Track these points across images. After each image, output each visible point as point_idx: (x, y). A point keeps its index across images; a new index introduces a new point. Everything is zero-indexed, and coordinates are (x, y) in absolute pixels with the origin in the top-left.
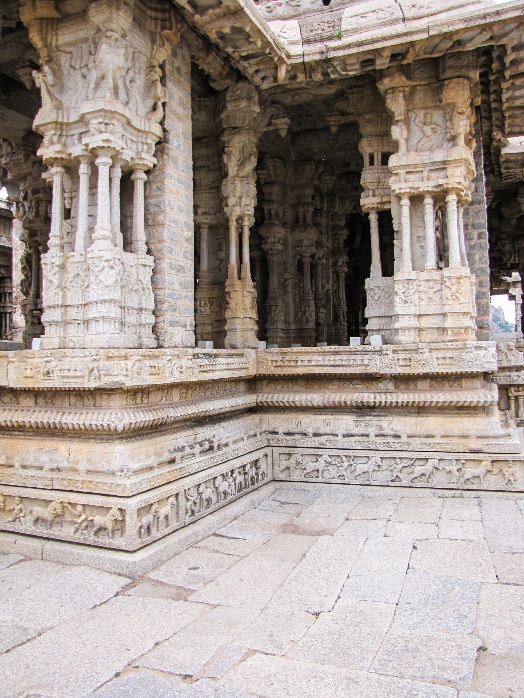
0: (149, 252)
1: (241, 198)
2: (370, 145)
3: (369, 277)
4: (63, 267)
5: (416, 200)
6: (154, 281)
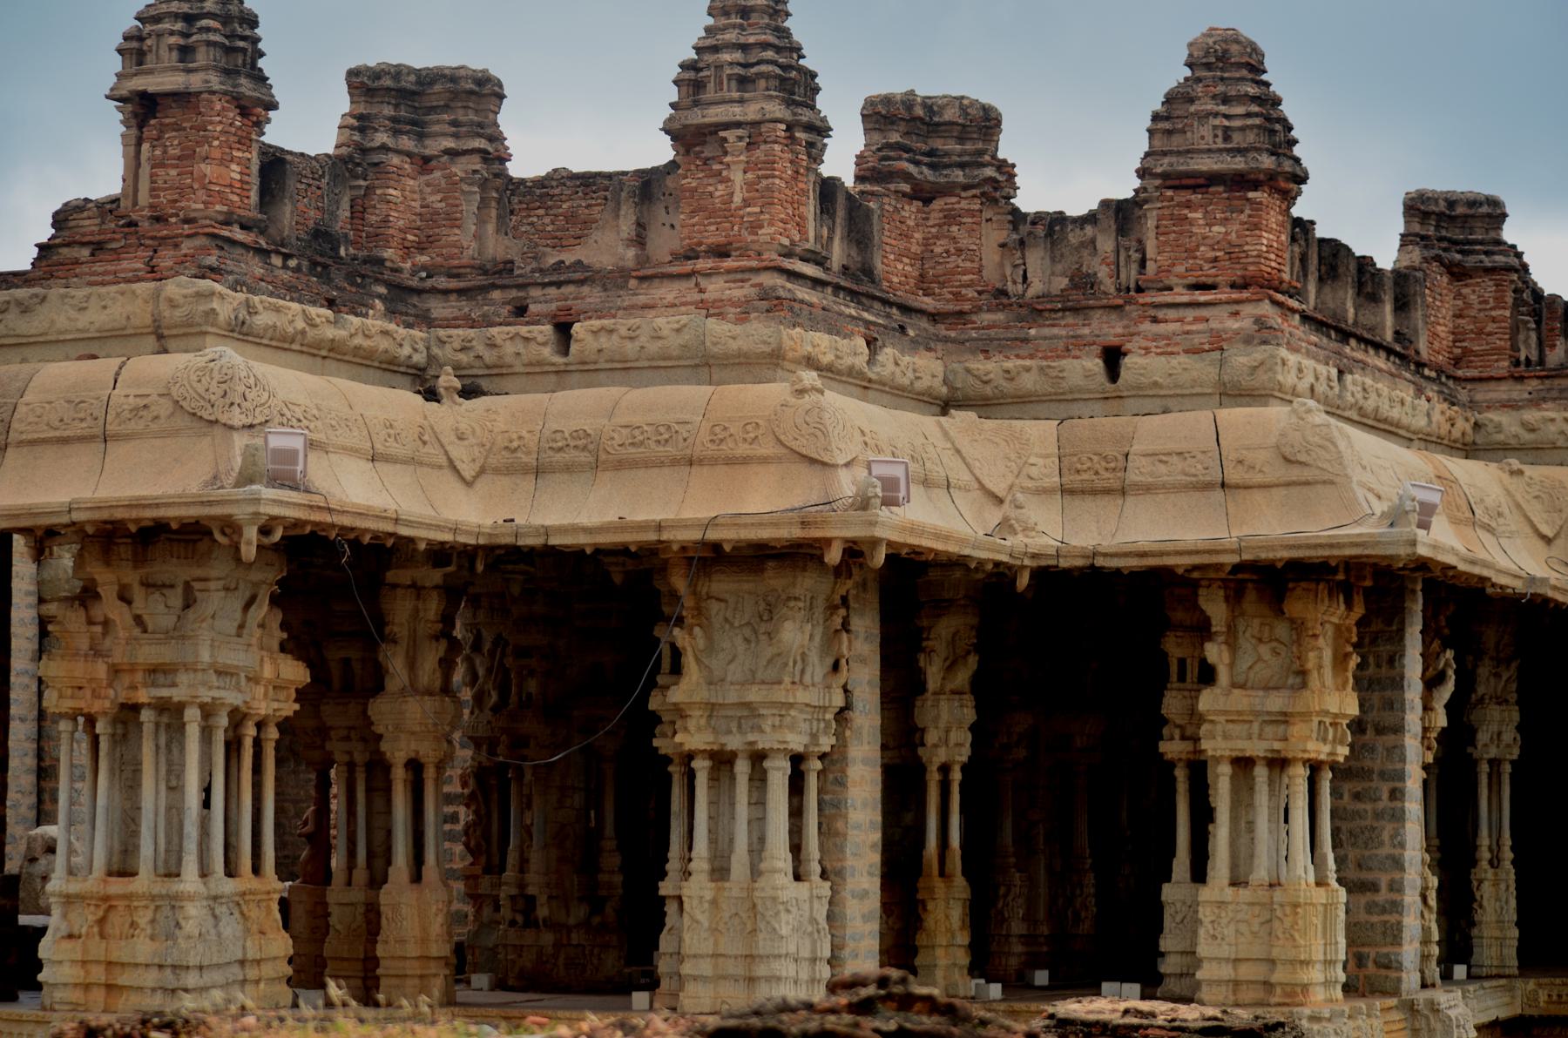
0: (824, 875)
1: (948, 731)
2: (1179, 645)
3: (1169, 880)
4: (714, 902)
5: (1243, 764)
6: (830, 917)
